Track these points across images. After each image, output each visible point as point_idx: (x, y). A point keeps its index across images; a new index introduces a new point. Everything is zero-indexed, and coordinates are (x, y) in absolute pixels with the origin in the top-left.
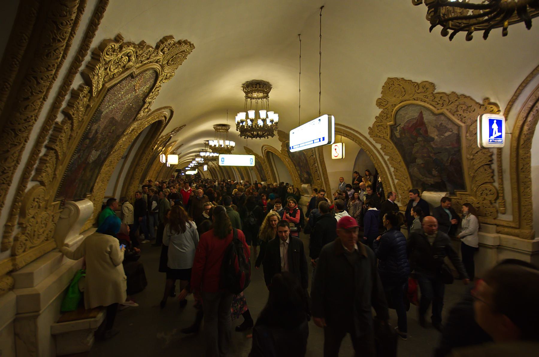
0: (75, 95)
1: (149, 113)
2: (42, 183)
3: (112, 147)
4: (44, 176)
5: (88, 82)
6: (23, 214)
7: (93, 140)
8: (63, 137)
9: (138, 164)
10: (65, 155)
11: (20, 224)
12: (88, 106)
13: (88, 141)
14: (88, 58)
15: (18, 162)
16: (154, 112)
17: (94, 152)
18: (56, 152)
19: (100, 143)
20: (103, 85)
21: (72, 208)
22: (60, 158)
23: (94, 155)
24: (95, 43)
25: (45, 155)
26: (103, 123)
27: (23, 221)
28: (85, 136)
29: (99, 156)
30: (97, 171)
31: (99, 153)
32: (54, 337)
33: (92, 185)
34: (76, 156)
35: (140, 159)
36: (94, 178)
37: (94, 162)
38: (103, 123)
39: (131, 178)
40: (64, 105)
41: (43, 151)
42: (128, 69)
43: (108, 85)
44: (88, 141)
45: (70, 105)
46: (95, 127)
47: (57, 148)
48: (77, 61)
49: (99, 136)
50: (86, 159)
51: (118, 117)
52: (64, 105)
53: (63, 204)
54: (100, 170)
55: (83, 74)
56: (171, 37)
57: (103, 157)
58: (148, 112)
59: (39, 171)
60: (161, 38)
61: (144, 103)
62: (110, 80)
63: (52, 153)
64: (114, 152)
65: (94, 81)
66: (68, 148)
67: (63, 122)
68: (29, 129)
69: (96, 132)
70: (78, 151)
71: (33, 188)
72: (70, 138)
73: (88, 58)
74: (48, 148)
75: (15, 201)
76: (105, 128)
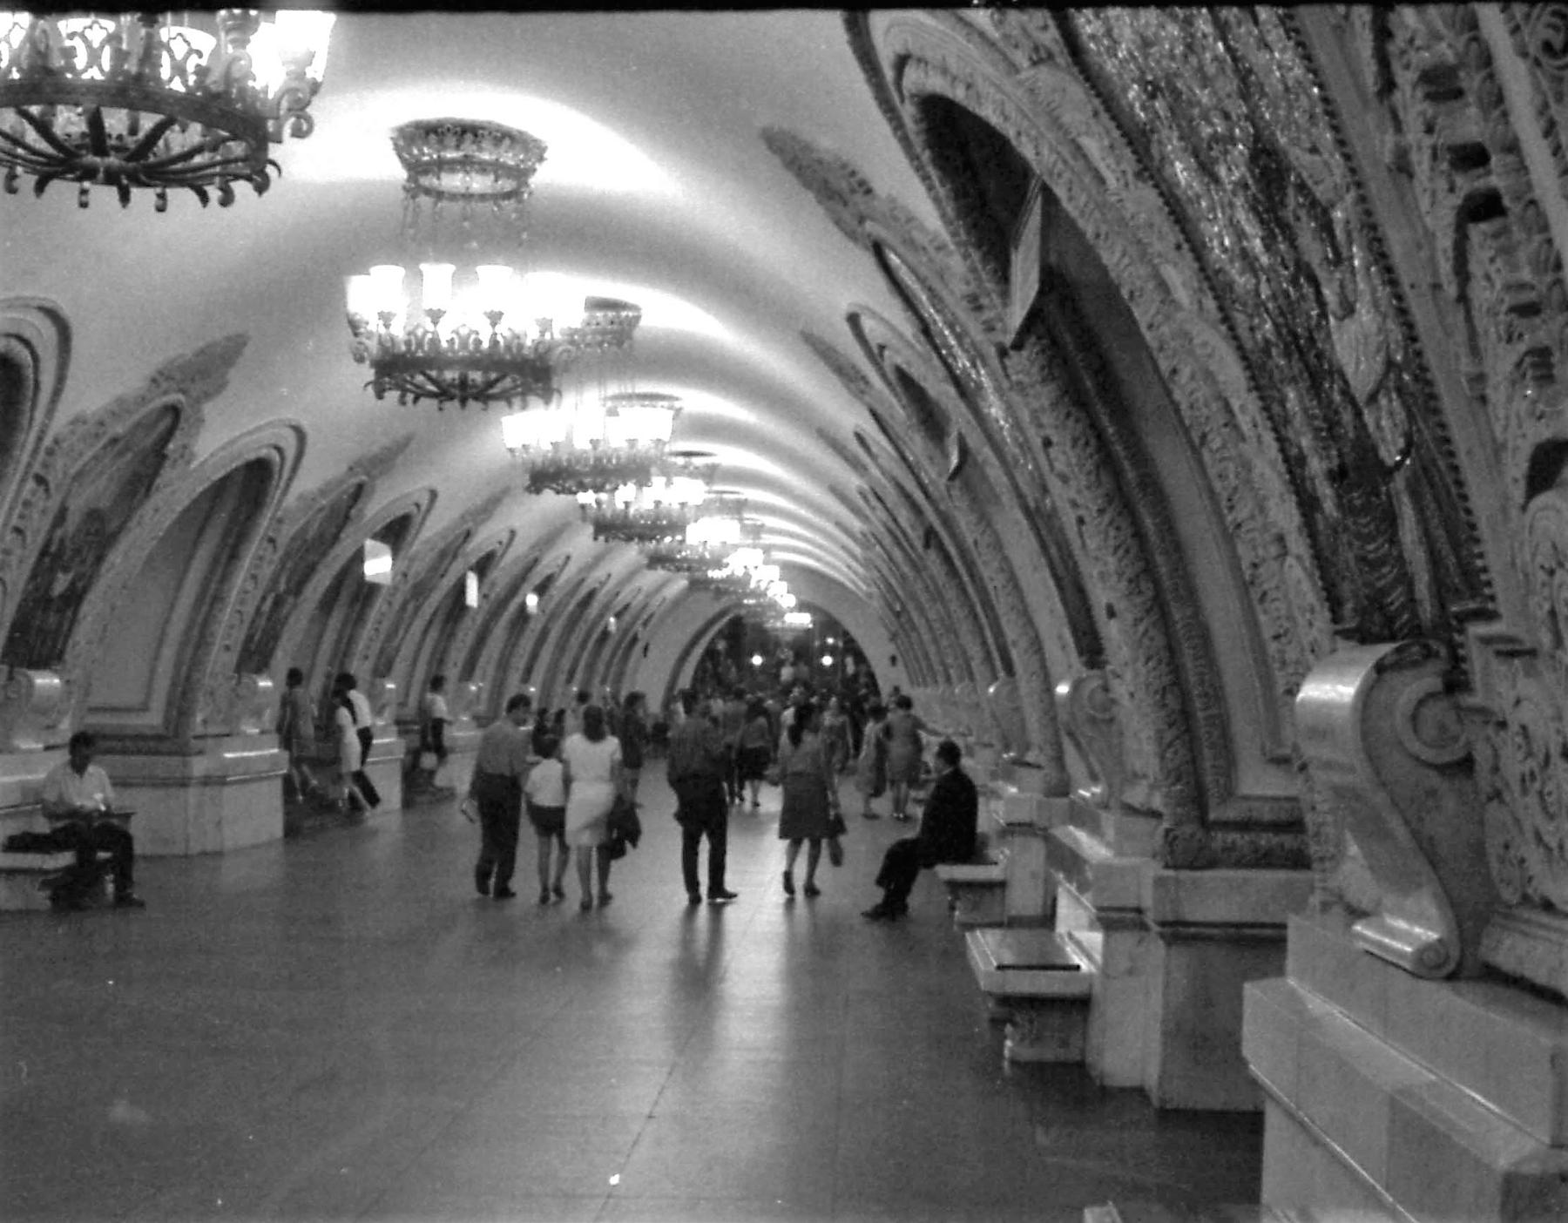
0: (27, 504)
1: (193, 466)
3: (100, 559)
7: (58, 556)
9: (218, 599)
13: (47, 560)
17: (60, 575)
20: (65, 473)
23: (61, 583)
24: (48, 441)
28: (44, 552)
29: (73, 583)
30: (69, 613)
31: (70, 576)
37: (61, 596)
39: (198, 647)
43: (72, 471)
44: (50, 559)
46: (59, 533)
49: (68, 543)
51: (104, 504)
54: (75, 613)
57: (80, 585)
58: (188, 463)
61: (164, 457)
69: (62, 541)
70: (34, 576)
76: (79, 530)
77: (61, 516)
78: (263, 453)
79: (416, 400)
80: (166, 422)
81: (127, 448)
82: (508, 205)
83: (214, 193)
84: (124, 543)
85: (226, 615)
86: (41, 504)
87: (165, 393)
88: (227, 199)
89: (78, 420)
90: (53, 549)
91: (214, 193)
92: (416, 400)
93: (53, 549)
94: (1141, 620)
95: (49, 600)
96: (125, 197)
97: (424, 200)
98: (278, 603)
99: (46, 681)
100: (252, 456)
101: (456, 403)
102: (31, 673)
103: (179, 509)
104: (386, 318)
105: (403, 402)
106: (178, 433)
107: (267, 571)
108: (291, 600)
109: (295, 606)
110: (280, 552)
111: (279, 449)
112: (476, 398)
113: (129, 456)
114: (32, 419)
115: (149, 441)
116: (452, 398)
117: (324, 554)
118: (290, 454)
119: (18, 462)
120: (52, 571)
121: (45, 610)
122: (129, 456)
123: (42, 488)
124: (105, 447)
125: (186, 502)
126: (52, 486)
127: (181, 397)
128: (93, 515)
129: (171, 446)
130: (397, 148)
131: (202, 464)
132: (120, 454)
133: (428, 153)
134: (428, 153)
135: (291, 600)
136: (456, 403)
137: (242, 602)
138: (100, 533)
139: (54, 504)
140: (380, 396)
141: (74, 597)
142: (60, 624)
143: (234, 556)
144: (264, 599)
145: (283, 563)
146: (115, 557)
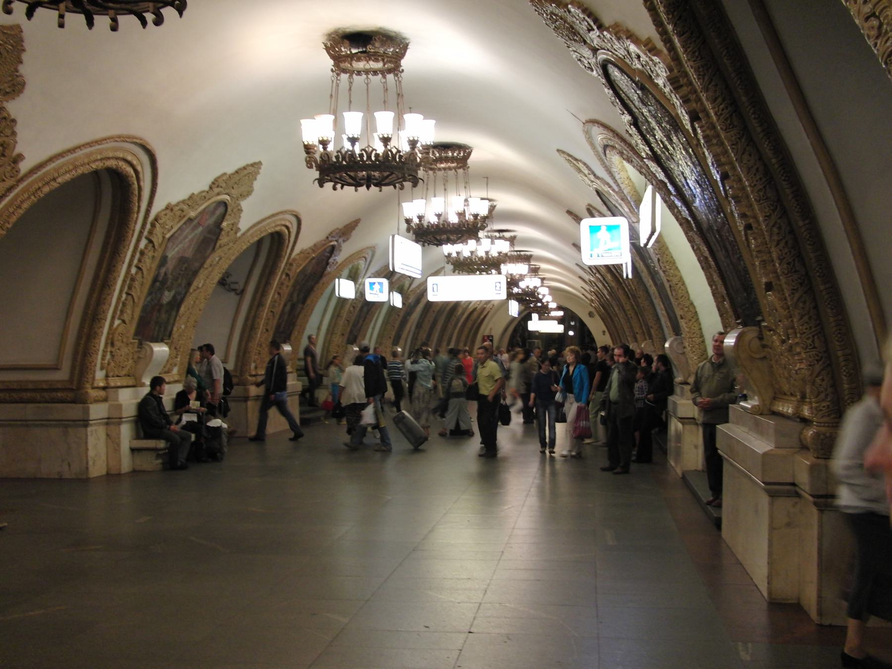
0: (142, 253)
1: (239, 234)
2: (124, 322)
3: (189, 284)
4: (126, 317)
5: (151, 241)
6: (112, 344)
7: (164, 282)
8: (137, 284)
9: (261, 304)
10: (139, 298)
11: (111, 352)
12: (153, 257)
13: (158, 284)
14: (148, 226)
15: (110, 305)
16: (248, 230)
17: (166, 293)
18: (132, 297)
19: (172, 283)
20: (164, 237)
21: (148, 349)
22: (136, 300)
23: (167, 296)
25: (126, 299)
26: (170, 265)
27: (113, 350)
28: (155, 280)
29: (174, 297)
30: (174, 313)
31: (173, 293)
32: (133, 450)
33: (169, 328)
34: (149, 299)
35: (264, 294)
36: (172, 321)
37: (170, 303)
38: (170, 265)
40: (135, 261)
41: (124, 296)
42: (184, 216)
43: (168, 236)
44: (159, 284)
45: (140, 261)
46: (163, 270)
47: (133, 294)
48: (141, 233)
49: (170, 276)
50: (159, 300)
51: (189, 254)
52: (135, 261)
53: (140, 344)
54: (178, 311)
55: (147, 238)
56: (225, 174)
57: (179, 298)
58: (236, 233)
59: (122, 312)
60: (212, 180)
61: (221, 230)
62: (169, 231)
63: (130, 297)
64: (195, 290)
65: (154, 240)
66: (141, 292)
67: (136, 273)
68: (115, 284)
69: (166, 274)
70: (150, 293)
71: (119, 325)
72: (142, 284)
73: (148, 226)
74: (128, 294)
75: (108, 333)
77: (164, 260)
78: (278, 229)
79: (342, 188)
80: (221, 210)
81: (199, 224)
82: (390, 77)
83: (150, 17)
84: (202, 275)
85: (265, 313)
86: (151, 254)
87: (218, 194)
88: (159, 21)
89: (169, 208)
90: (160, 279)
91: (150, 17)
92: (342, 188)
93: (160, 279)
94: (797, 290)
95: (162, 306)
96: (90, 23)
97: (344, 77)
98: (293, 307)
99: (161, 350)
100: (273, 230)
101: (364, 187)
102: (152, 344)
103: (233, 258)
104: (324, 143)
105: (335, 188)
106: (227, 217)
107: (286, 291)
108: (300, 306)
109: (302, 308)
110: (292, 281)
111: (287, 227)
112: (376, 185)
113: (200, 229)
114: (139, 207)
115: (211, 221)
116: (361, 185)
117: (317, 282)
118: (294, 231)
119: (134, 231)
120: (161, 290)
121: (159, 311)
122: (200, 229)
123: (151, 245)
124: (185, 223)
125: (237, 254)
126: (156, 244)
127: (228, 197)
128: (182, 260)
129: (224, 224)
130: (327, 49)
131: (244, 234)
132: (195, 228)
133: (345, 50)
134: (345, 50)
135: (300, 306)
136: (364, 187)
137: (274, 306)
138: (188, 271)
139: (158, 254)
140: (321, 186)
141: (176, 304)
142: (169, 319)
143: (268, 284)
144: (285, 305)
145: (294, 286)
146: (198, 282)
